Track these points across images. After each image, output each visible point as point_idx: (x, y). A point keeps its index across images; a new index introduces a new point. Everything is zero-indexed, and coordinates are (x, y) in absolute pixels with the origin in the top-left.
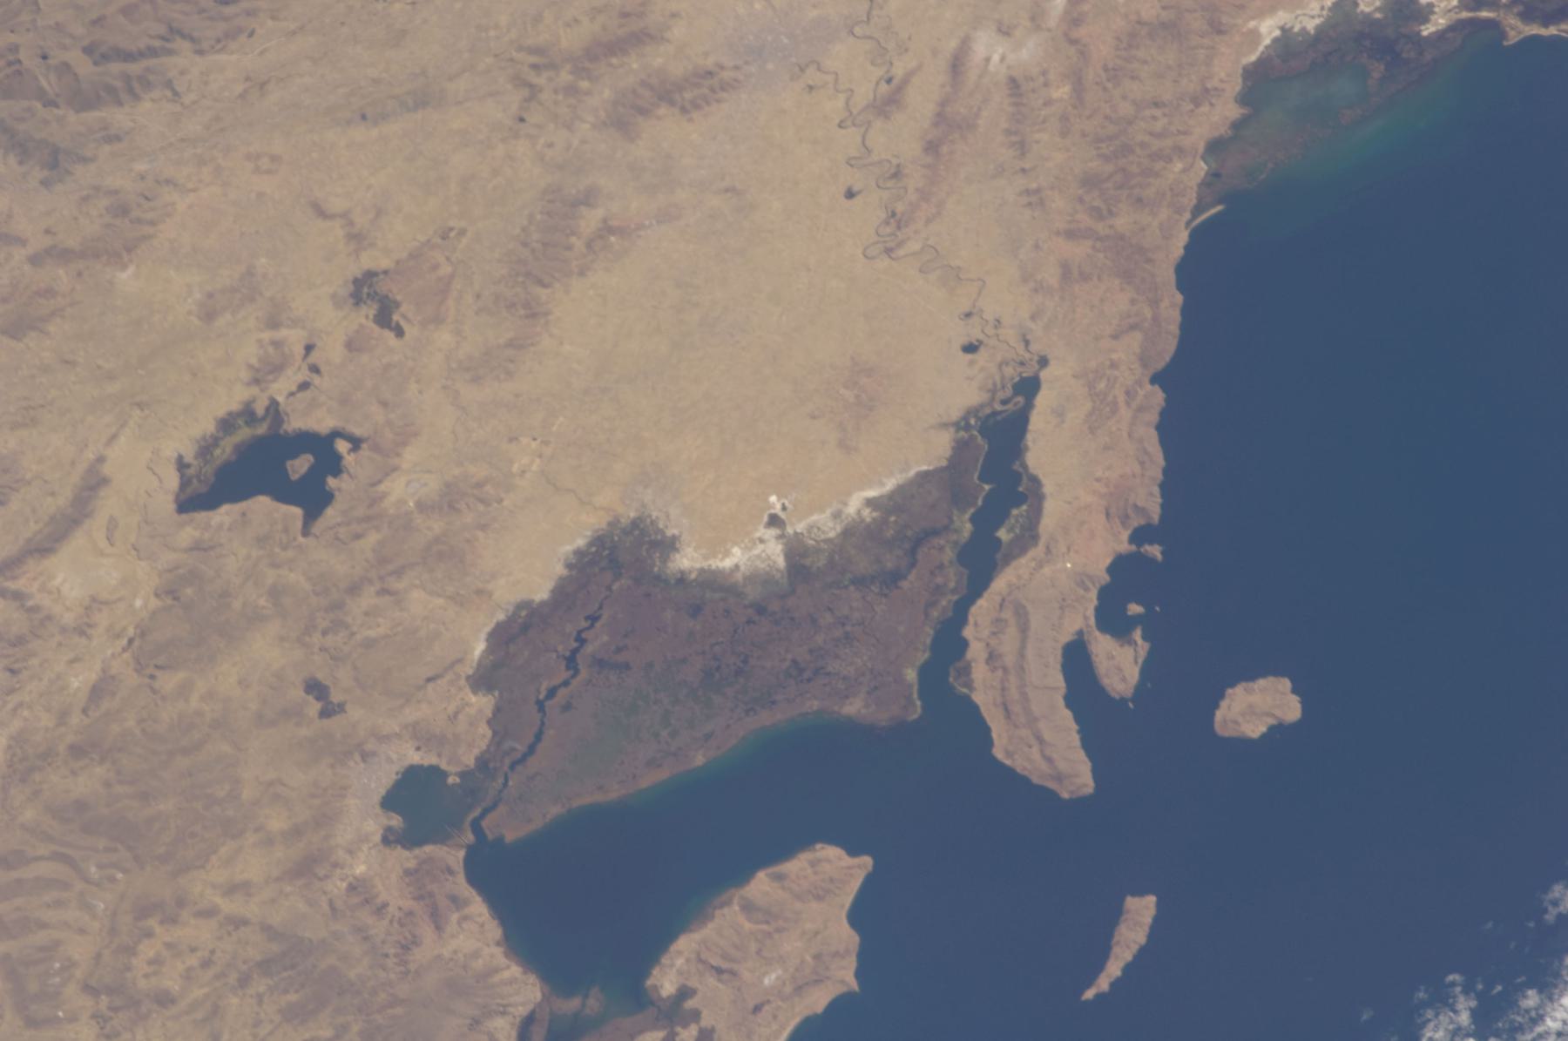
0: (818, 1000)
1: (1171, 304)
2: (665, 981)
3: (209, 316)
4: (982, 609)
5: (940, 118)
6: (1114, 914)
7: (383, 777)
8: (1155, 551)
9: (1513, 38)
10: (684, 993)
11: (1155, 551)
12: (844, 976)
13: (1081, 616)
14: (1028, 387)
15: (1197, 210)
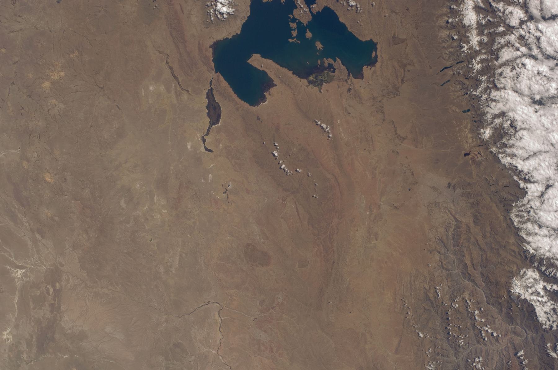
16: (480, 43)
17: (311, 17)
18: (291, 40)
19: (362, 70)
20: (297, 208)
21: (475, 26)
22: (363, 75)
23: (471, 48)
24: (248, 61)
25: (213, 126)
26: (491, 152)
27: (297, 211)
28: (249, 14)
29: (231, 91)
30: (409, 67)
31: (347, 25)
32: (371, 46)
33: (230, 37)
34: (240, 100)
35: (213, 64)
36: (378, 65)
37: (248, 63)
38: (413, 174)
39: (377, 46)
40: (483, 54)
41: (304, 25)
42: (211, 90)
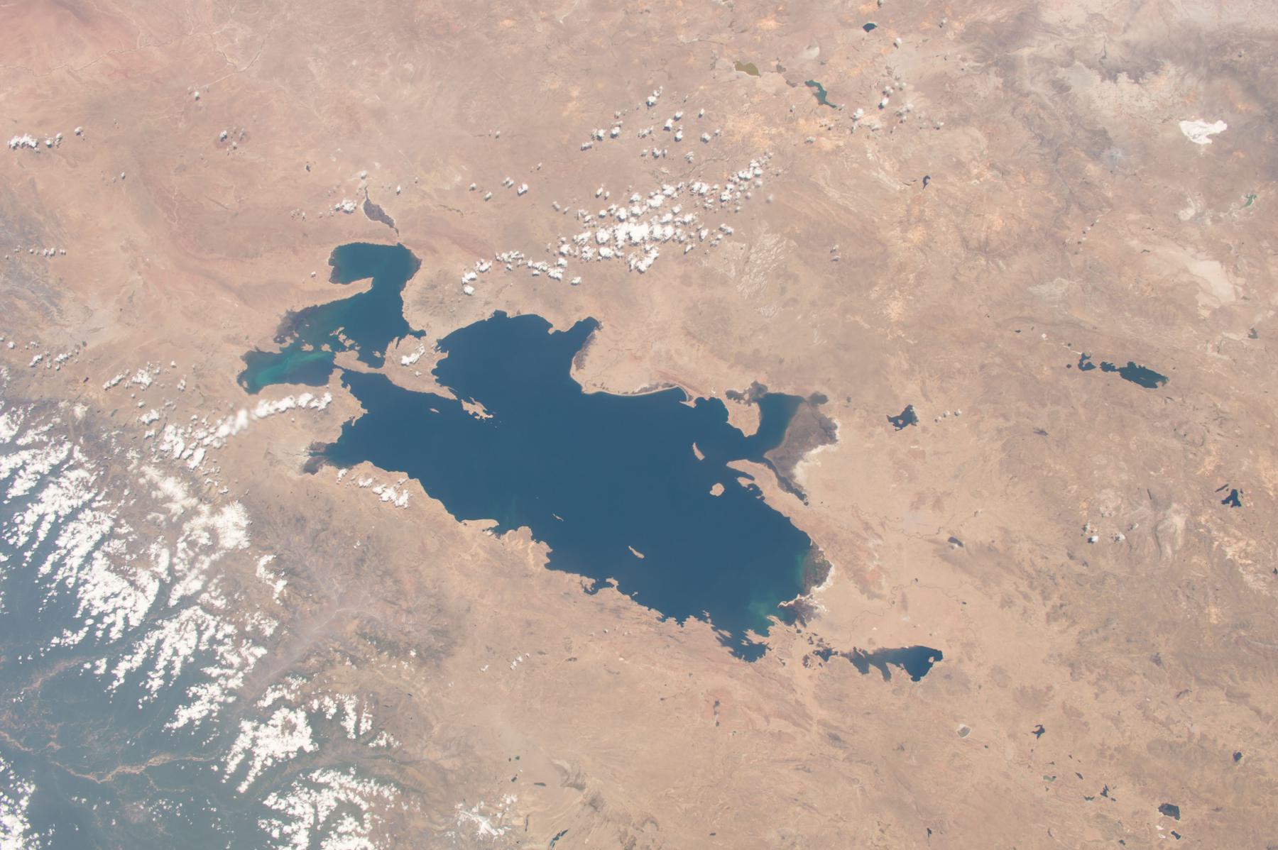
0: (730, 417)
1: (800, 527)
2: (755, 407)
3: (945, 430)
4: (773, 474)
5: (871, 528)
6: (703, 453)
7: (829, 398)
8: (758, 497)
9: (799, 595)
10: (750, 405)
11: (758, 497)
12: (730, 422)
13: (757, 482)
14: (806, 504)
15: (814, 542)
16: (143, 475)
17: (335, 363)
18: (341, 329)
19: (247, 363)
20: (223, 206)
21: (161, 485)
22: (243, 360)
23: (150, 463)
24: (371, 279)
25: (365, 200)
26: (63, 400)
27: (219, 204)
28: (404, 315)
29: (371, 241)
30: (201, 401)
31: (292, 386)
32: (254, 389)
33: (408, 283)
34: (354, 242)
35: (407, 247)
36: (234, 379)
37: (370, 277)
38: (128, 324)
39: (247, 394)
40: (134, 469)
41: (338, 351)
42: (391, 225)
